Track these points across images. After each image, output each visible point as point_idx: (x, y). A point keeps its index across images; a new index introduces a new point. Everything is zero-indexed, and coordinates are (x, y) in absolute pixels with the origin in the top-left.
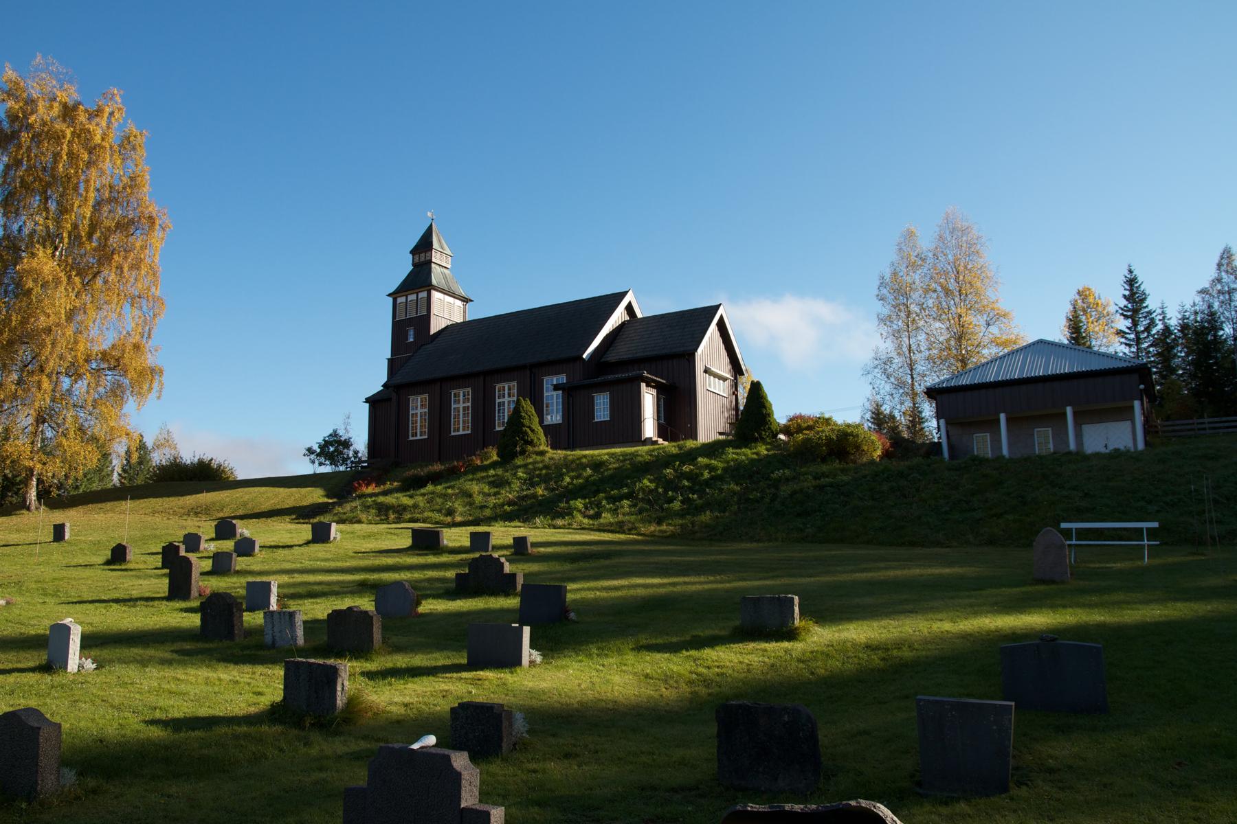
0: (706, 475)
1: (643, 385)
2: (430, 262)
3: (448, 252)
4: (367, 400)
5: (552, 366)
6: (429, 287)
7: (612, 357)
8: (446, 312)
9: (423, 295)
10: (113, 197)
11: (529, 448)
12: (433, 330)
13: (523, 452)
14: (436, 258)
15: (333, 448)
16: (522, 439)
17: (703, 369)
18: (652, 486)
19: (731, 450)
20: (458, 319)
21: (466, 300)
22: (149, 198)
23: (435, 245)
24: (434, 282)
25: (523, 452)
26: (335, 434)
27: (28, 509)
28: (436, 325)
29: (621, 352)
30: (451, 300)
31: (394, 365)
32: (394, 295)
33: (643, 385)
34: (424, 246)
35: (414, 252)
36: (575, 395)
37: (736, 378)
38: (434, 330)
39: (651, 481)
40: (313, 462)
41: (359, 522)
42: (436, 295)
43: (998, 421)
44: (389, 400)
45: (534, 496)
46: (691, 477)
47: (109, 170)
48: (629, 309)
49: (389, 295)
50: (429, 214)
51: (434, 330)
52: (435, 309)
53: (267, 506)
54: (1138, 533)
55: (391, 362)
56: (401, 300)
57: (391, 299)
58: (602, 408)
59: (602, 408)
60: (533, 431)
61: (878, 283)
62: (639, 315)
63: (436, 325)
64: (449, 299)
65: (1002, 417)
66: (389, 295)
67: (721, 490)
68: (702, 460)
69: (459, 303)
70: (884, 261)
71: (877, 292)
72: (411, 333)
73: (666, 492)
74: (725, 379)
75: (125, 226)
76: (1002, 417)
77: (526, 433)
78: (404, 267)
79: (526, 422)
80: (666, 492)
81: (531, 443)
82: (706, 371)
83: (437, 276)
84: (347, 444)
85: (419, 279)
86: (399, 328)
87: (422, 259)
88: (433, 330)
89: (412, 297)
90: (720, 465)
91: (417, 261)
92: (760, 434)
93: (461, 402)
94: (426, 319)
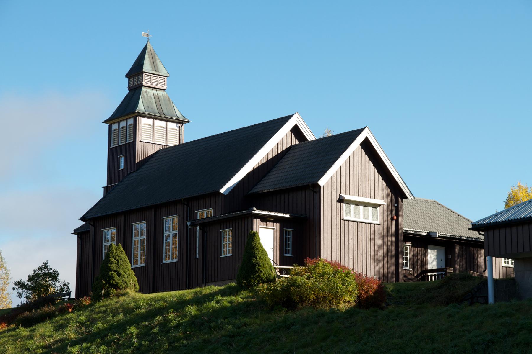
1: (257, 223)
2: (141, 86)
3: (163, 72)
4: (76, 232)
8: (153, 136)
9: (131, 121)
11: (114, 291)
14: (146, 80)
16: (107, 282)
17: (335, 198)
20: (173, 142)
21: (181, 122)
23: (147, 66)
25: (107, 295)
26: (45, 265)
30: (163, 123)
32: (109, 122)
33: (257, 223)
34: (136, 72)
35: (129, 75)
37: (397, 202)
38: (140, 157)
40: (20, 296)
42: (144, 123)
44: (89, 231)
48: (296, 131)
49: (105, 122)
50: (144, 34)
51: (140, 157)
55: (106, 189)
56: (115, 127)
57: (107, 126)
60: (119, 274)
62: (310, 137)
66: (105, 122)
72: (122, 160)
74: (375, 206)
77: (112, 277)
81: (116, 286)
82: (341, 200)
84: (54, 276)
86: (114, 154)
87: (136, 83)
89: (123, 124)
92: (249, 283)
94: (130, 148)
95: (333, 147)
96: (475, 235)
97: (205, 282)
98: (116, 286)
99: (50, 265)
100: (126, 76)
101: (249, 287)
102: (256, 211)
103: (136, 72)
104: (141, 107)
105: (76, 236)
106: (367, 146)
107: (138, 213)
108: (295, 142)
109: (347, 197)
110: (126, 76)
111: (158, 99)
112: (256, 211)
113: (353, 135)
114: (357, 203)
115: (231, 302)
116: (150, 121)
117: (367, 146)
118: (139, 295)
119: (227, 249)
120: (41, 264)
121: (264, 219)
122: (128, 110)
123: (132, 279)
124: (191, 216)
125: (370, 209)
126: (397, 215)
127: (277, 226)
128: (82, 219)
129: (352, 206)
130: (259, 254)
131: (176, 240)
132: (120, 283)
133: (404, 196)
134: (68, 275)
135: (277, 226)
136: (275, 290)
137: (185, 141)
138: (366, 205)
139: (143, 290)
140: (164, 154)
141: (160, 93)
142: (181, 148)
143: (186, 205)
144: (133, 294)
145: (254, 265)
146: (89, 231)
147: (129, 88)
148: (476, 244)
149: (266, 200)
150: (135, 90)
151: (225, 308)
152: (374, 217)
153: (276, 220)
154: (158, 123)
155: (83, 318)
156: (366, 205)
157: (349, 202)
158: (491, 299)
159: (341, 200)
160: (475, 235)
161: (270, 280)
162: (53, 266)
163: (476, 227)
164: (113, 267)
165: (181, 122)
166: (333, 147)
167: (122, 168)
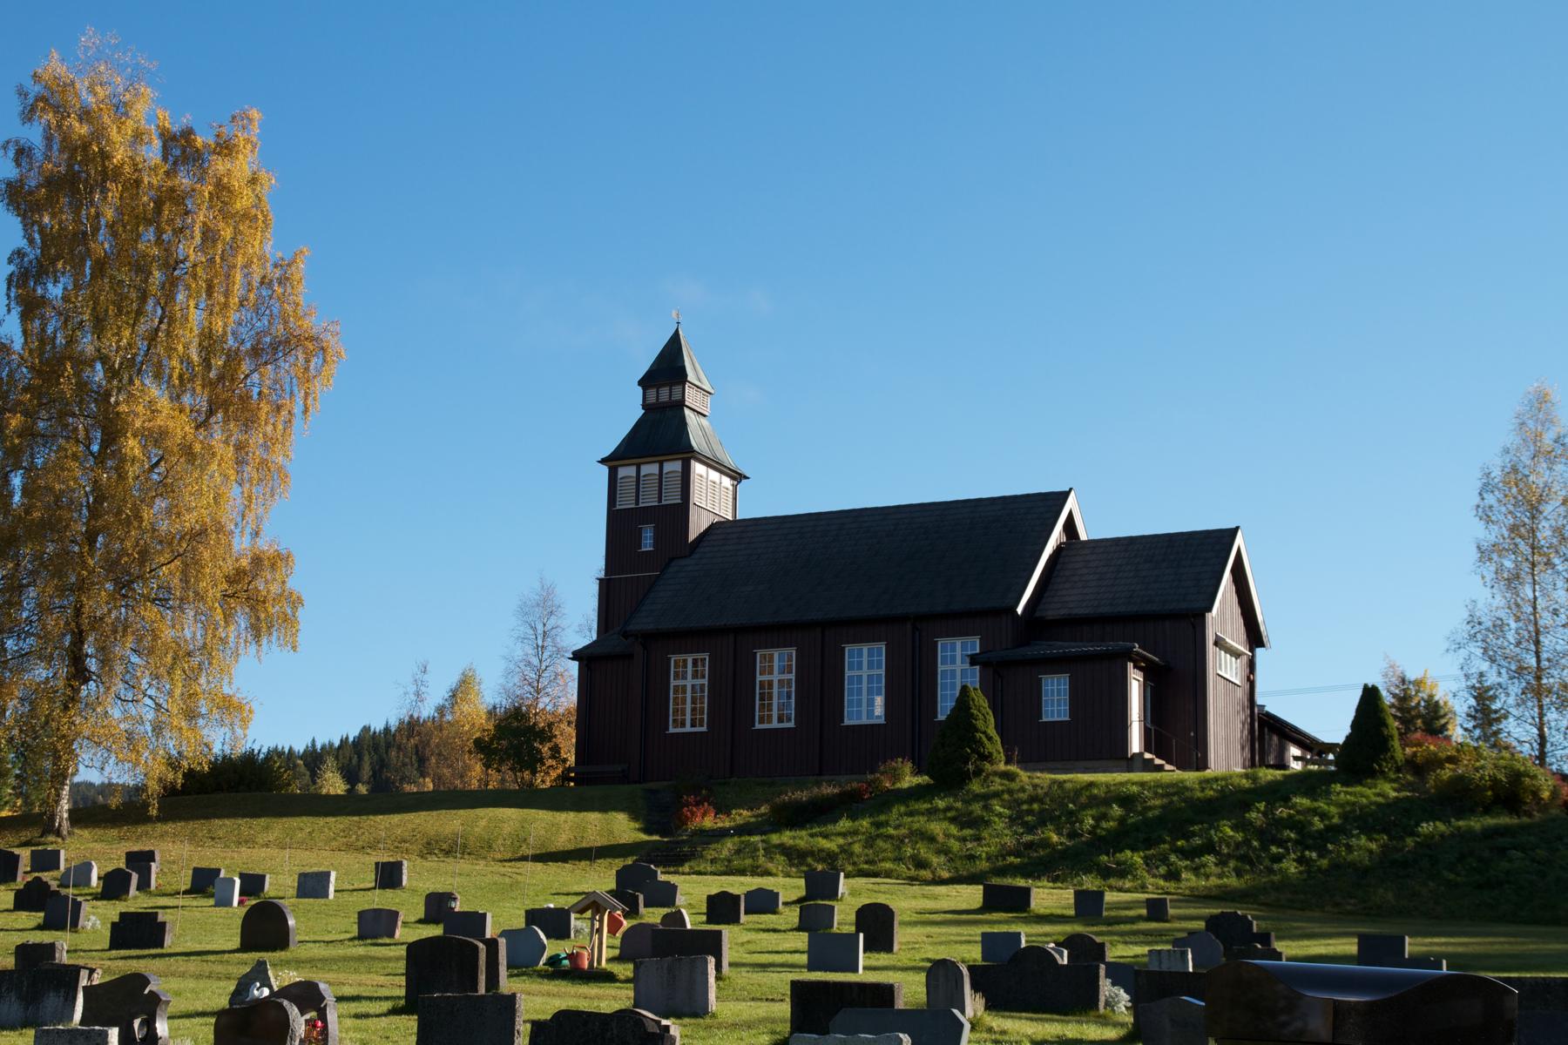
0: (1318, 824)
1: (1130, 665)
2: (681, 404)
5: (957, 621)
7: (1052, 611)
9: (674, 466)
11: (987, 766)
12: (692, 536)
13: (978, 772)
18: (1239, 837)
19: (1338, 787)
21: (737, 477)
24: (696, 440)
25: (978, 772)
27: (58, 833)
28: (698, 524)
29: (1072, 601)
31: (614, 595)
32: (612, 461)
33: (1130, 665)
35: (646, 382)
36: (1007, 674)
39: (1234, 828)
41: (768, 873)
42: (698, 469)
44: (629, 657)
45: (1045, 843)
46: (1290, 823)
49: (603, 461)
52: (698, 496)
53: (562, 842)
57: (605, 470)
58: (1056, 699)
59: (1056, 699)
61: (1479, 484)
63: (698, 524)
64: (714, 475)
66: (603, 461)
67: (1349, 848)
68: (1302, 802)
69: (727, 482)
70: (1490, 444)
71: (1477, 500)
73: (1265, 848)
75: (266, 351)
77: (982, 744)
78: (627, 411)
79: (980, 724)
80: (1265, 848)
82: (1218, 643)
83: (698, 430)
85: (660, 434)
86: (621, 526)
88: (692, 536)
89: (650, 469)
90: (1333, 810)
91: (652, 399)
93: (777, 670)
100: (641, 383)
105: (576, 664)
107: (775, 633)
110: (641, 383)
133: (1261, 645)
142: (736, 523)
146: (630, 656)
147: (644, 406)
167: (647, 545)
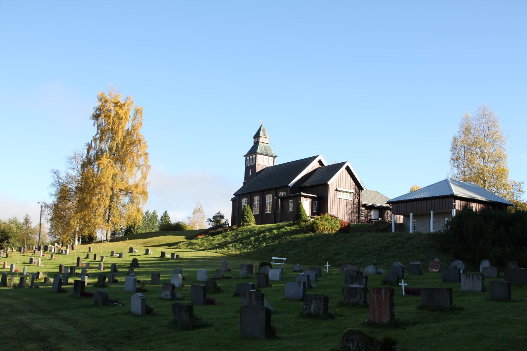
1: (302, 198)
2: (259, 142)
3: (268, 136)
4: (232, 200)
6: (256, 153)
8: (263, 163)
9: (254, 156)
10: (129, 133)
11: (245, 223)
14: (261, 140)
15: (217, 218)
16: (243, 220)
20: (271, 165)
22: (143, 132)
23: (261, 134)
25: (243, 225)
26: (219, 213)
30: (267, 157)
32: (246, 156)
33: (302, 198)
34: (257, 136)
35: (254, 138)
38: (257, 170)
43: (430, 214)
47: (128, 125)
48: (320, 162)
51: (257, 170)
54: (281, 261)
55: (244, 183)
56: (248, 158)
60: (248, 217)
62: (326, 164)
65: (432, 212)
70: (455, 130)
74: (350, 193)
76: (432, 212)
77: (245, 218)
78: (252, 144)
81: (246, 222)
82: (337, 190)
84: (223, 217)
86: (247, 169)
89: (251, 157)
94: (254, 167)
95: (335, 168)
96: (388, 205)
97: (282, 221)
98: (246, 222)
99: (221, 212)
101: (298, 223)
102: (302, 194)
103: (257, 136)
104: (258, 150)
106: (348, 169)
107: (256, 193)
108: (320, 166)
109: (339, 189)
111: (265, 147)
112: (302, 194)
113: (342, 164)
114: (343, 192)
115: (290, 229)
116: (262, 156)
117: (348, 169)
118: (256, 225)
119: (291, 209)
120: (218, 212)
121: (306, 197)
122: (253, 151)
123: (253, 219)
124: (277, 195)
125: (349, 194)
126: (359, 196)
127: (310, 200)
128: (234, 195)
129: (341, 193)
130: (302, 211)
131: (271, 204)
132: (248, 220)
133: (362, 189)
134: (228, 217)
135: (310, 200)
136: (308, 225)
137: (275, 165)
138: (347, 192)
139: (257, 224)
140: (267, 170)
141: (266, 145)
143: (275, 191)
144: (253, 225)
145: (300, 215)
148: (386, 208)
149: (307, 189)
150: (256, 144)
151: (288, 231)
152: (349, 197)
153: (310, 197)
154: (265, 156)
155: (233, 233)
156: (347, 192)
157: (340, 191)
158: (393, 231)
159: (337, 190)
160: (388, 205)
161: (307, 221)
162: (222, 213)
163: (388, 203)
164: (246, 214)
165: (275, 157)
166: (335, 168)
